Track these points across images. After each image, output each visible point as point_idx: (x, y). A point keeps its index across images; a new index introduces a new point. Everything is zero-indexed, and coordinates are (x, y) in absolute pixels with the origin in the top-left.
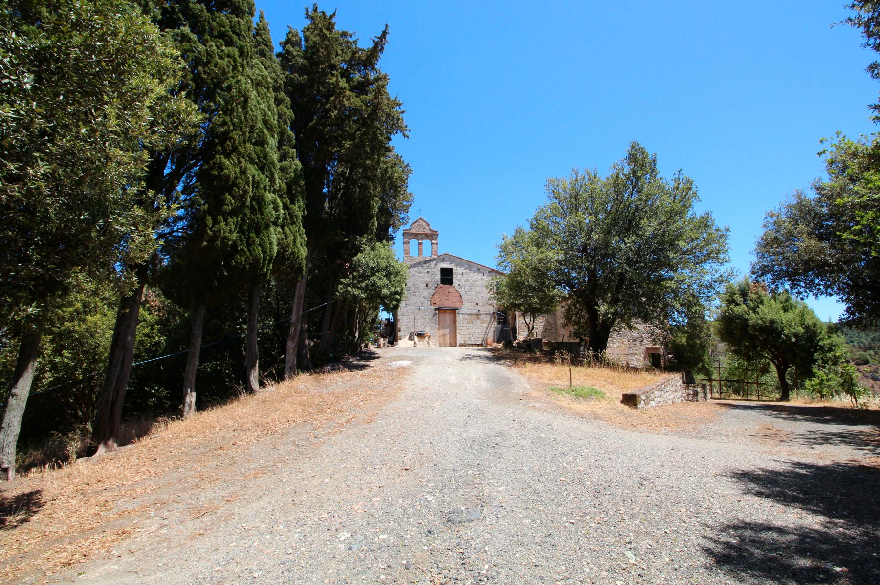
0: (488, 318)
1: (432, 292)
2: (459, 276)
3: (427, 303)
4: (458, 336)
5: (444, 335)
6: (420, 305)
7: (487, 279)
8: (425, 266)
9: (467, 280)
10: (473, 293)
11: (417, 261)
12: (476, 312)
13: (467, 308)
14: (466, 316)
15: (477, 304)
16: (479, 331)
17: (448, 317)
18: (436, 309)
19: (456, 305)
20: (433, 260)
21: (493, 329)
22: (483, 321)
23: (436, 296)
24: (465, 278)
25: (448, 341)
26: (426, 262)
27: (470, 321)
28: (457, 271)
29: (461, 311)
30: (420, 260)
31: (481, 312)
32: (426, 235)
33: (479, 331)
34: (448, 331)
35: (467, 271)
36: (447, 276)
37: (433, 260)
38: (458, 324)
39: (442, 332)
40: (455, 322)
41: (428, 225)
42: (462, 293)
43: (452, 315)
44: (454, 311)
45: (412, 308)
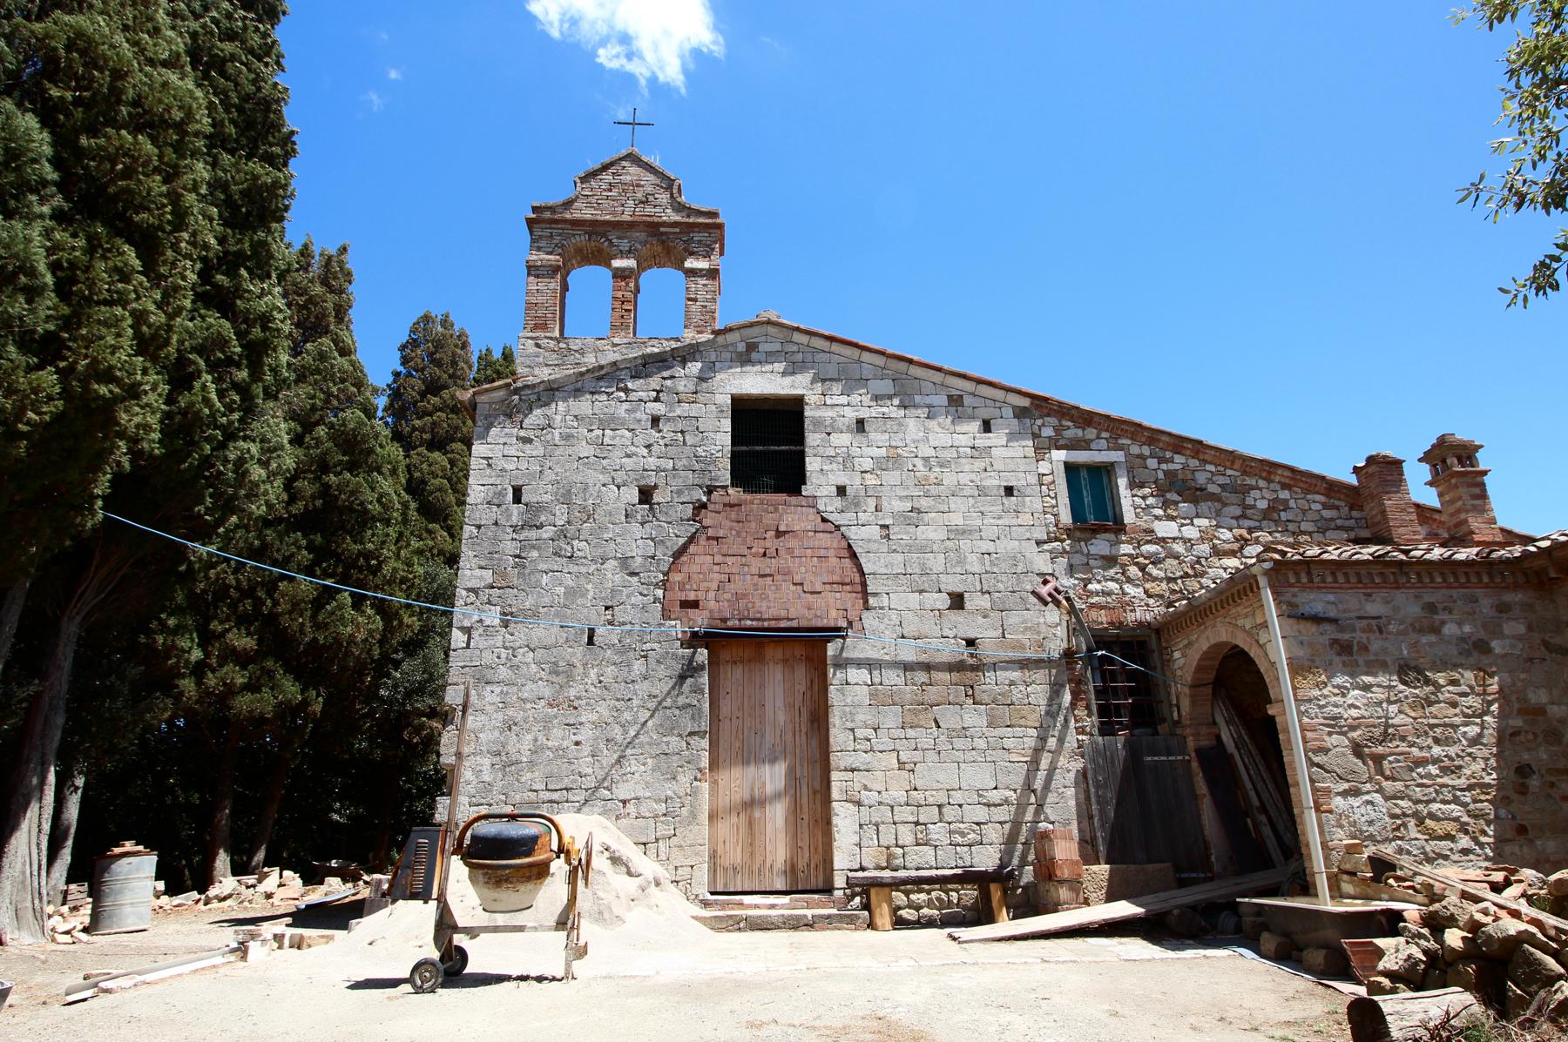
2: (842, 440)
3: (638, 604)
4: (844, 820)
5: (752, 804)
6: (597, 618)
7: (1010, 454)
8: (641, 388)
9: (892, 460)
10: (931, 533)
11: (590, 360)
12: (964, 653)
14: (893, 677)
15: (957, 601)
16: (978, 776)
17: (775, 690)
19: (829, 609)
20: (684, 355)
21: (1070, 767)
22: (1002, 712)
23: (701, 560)
25: (777, 850)
26: (647, 366)
27: (919, 711)
28: (830, 411)
29: (857, 647)
30: (611, 356)
31: (988, 651)
32: (653, 228)
33: (978, 776)
34: (773, 777)
35: (892, 409)
36: (769, 446)
37: (684, 355)
39: (736, 782)
41: (668, 184)
42: (863, 534)
43: (801, 673)
44: (809, 649)
45: (544, 632)
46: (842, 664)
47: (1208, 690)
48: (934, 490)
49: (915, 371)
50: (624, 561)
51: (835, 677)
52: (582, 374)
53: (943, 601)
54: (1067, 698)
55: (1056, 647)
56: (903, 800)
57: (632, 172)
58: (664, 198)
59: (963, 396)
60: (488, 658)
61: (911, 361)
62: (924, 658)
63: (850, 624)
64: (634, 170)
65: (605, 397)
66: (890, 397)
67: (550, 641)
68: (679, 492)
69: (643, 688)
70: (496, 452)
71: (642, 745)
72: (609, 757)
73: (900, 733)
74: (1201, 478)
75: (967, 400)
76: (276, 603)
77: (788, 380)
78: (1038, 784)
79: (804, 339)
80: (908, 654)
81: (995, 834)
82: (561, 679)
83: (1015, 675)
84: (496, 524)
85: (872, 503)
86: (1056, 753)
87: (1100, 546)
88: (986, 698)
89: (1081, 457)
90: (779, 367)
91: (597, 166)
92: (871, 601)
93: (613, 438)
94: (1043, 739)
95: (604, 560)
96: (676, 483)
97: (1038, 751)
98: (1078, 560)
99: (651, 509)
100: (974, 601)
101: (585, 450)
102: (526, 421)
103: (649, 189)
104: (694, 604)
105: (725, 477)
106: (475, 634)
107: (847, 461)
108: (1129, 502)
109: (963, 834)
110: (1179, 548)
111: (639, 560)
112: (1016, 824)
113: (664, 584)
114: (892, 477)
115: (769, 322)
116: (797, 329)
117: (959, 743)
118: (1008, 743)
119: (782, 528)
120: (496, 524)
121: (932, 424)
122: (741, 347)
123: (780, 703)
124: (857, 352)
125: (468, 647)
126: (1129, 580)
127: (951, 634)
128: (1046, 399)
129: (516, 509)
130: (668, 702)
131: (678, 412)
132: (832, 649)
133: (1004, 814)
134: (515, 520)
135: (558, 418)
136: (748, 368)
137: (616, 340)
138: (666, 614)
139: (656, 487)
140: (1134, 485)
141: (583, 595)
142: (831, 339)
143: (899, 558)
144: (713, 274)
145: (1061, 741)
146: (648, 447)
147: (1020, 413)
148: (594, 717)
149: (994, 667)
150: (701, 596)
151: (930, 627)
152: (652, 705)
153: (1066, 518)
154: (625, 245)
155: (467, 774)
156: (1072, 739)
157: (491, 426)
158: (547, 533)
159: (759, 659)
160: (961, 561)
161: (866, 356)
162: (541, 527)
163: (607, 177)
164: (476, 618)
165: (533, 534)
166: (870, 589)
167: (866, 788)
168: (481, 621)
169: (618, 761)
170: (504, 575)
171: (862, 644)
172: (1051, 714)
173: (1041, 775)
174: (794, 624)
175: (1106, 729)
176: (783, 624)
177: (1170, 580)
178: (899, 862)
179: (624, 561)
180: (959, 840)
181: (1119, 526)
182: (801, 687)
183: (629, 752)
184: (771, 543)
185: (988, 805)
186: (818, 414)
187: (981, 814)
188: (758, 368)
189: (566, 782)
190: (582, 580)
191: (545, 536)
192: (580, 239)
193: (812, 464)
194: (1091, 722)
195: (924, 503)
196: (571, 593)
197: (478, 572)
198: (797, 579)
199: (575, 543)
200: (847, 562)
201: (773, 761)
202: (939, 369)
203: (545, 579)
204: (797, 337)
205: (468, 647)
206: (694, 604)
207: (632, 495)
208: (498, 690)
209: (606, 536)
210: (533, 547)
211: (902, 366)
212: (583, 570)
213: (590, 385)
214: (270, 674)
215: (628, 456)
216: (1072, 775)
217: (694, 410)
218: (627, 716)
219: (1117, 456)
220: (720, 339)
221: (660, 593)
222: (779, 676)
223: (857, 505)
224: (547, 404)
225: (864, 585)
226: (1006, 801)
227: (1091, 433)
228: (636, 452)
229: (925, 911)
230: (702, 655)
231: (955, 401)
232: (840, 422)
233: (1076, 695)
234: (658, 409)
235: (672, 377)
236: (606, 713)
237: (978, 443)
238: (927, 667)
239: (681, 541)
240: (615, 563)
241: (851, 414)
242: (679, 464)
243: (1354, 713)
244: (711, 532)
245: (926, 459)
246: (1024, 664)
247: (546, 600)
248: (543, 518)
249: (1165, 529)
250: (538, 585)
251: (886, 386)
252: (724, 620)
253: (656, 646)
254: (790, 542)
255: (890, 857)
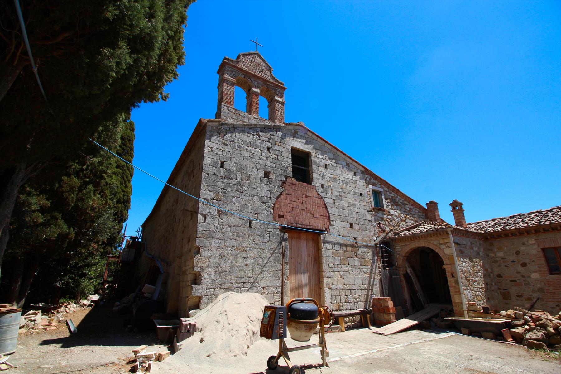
0: (369, 254)
1: (277, 191)
2: (322, 169)
3: (265, 213)
8: (265, 136)
9: (333, 180)
12: (351, 241)
13: (337, 232)
14: (337, 248)
16: (359, 281)
17: (305, 247)
18: (283, 229)
19: (318, 223)
21: (378, 277)
24: (329, 174)
28: (319, 159)
29: (329, 238)
31: (360, 242)
34: (304, 278)
35: (332, 163)
36: (302, 165)
38: (325, 267)
40: (317, 259)
41: (270, 69)
42: (328, 201)
43: (311, 244)
44: (315, 236)
45: (232, 220)
46: (325, 242)
47: (406, 258)
48: (345, 191)
49: (339, 153)
50: (261, 197)
51: (324, 246)
52: (245, 125)
53: (348, 226)
54: (376, 258)
55: (373, 243)
56: (342, 288)
57: (258, 60)
58: (268, 73)
59: (350, 164)
60: (213, 228)
61: (338, 150)
62: (345, 243)
63: (326, 229)
64: (258, 59)
65: (252, 136)
66: (333, 159)
67: (236, 224)
68: (278, 176)
69: (269, 245)
70: (214, 146)
71: (269, 267)
72: (258, 271)
73: (340, 266)
74: (397, 199)
75: (350, 165)
76: (61, 186)
77: (306, 146)
78: (371, 284)
79: (310, 134)
80: (341, 241)
81: (363, 298)
82: (240, 239)
83: (365, 250)
84: (215, 174)
85: (330, 191)
86: (375, 274)
87: (380, 214)
88: (359, 257)
89: (376, 188)
90: (304, 141)
91: (247, 53)
92: (332, 223)
93: (255, 151)
94: (372, 269)
95: (254, 196)
96: (276, 173)
97: (371, 273)
98: (376, 218)
99: (269, 180)
100: (356, 226)
101: (247, 154)
102: (225, 137)
103: (264, 68)
104: (282, 217)
105: (291, 174)
106: (207, 218)
107: (323, 177)
108: (386, 203)
109: (356, 299)
110: (395, 218)
111: (265, 198)
112: (367, 295)
113: (273, 208)
114: (334, 184)
115: (301, 126)
116: (309, 131)
117: (354, 270)
118: (365, 270)
119: (307, 195)
120: (215, 174)
121: (343, 170)
122: (293, 131)
123: (306, 254)
124: (324, 143)
125: (204, 222)
126: (386, 225)
127: (350, 235)
128: (368, 170)
129: (222, 170)
130: (276, 251)
131: (276, 148)
132: (322, 237)
133: (364, 292)
134: (222, 174)
135: (236, 139)
136: (295, 139)
137: (255, 117)
138: (274, 220)
139: (270, 172)
140: (386, 199)
141: (247, 208)
142: (318, 136)
143: (337, 210)
144: (283, 104)
145: (375, 270)
146: (267, 157)
147: (362, 172)
148: (252, 255)
149: (361, 247)
150: (284, 214)
151: (345, 233)
152: (271, 252)
153: (373, 205)
154: (256, 84)
155: (205, 276)
156: (378, 270)
157: (211, 136)
158: (234, 182)
159: (299, 238)
160: (352, 214)
161: (327, 145)
162: (232, 179)
163: (250, 58)
164: (208, 211)
165: (228, 181)
166: (331, 219)
167: (333, 284)
168: (210, 212)
169: (261, 272)
170: (218, 196)
171: (330, 236)
172: (373, 262)
173: (372, 280)
174: (311, 227)
175: (384, 268)
176: (308, 227)
177: (394, 226)
178: (341, 308)
179: (261, 197)
180: (355, 300)
181: (383, 210)
182: (311, 249)
183: (264, 269)
184: (304, 199)
185: (361, 289)
186: (315, 159)
187: (359, 292)
188: (298, 139)
189: (243, 280)
190: (247, 203)
191: (233, 183)
192: (241, 76)
193: (315, 176)
194: (381, 265)
195: (343, 194)
196: (244, 206)
197: (208, 192)
198: (312, 213)
199: (244, 187)
200: (325, 210)
201: (304, 273)
202: (344, 154)
203: (233, 199)
204: (309, 133)
205: (204, 222)
206: (282, 217)
207: (262, 174)
208: (217, 241)
209: (255, 187)
210: (229, 186)
211: (335, 150)
212: (247, 198)
213: (247, 130)
214: (56, 219)
215: (260, 159)
216: (378, 281)
217: (281, 148)
218: (264, 255)
219: (381, 190)
220: (287, 127)
221: (272, 211)
222: (305, 245)
223: (326, 191)
224: (232, 133)
225: (329, 217)
226: (365, 288)
227: (376, 182)
228: (262, 159)
229: (348, 324)
230: (286, 235)
231: (348, 165)
232: (321, 164)
233: (378, 257)
234: (269, 145)
235: (273, 135)
236: (256, 254)
237: (354, 179)
238: (346, 245)
239: (279, 193)
240: (257, 197)
241: (324, 162)
242: (277, 166)
243: (465, 269)
244: (287, 192)
245: (342, 181)
246: (367, 247)
247: (234, 208)
248: (232, 176)
249: (392, 212)
250: (231, 201)
251: (331, 156)
252: (292, 223)
253: (272, 230)
254: (309, 200)
255: (339, 306)
